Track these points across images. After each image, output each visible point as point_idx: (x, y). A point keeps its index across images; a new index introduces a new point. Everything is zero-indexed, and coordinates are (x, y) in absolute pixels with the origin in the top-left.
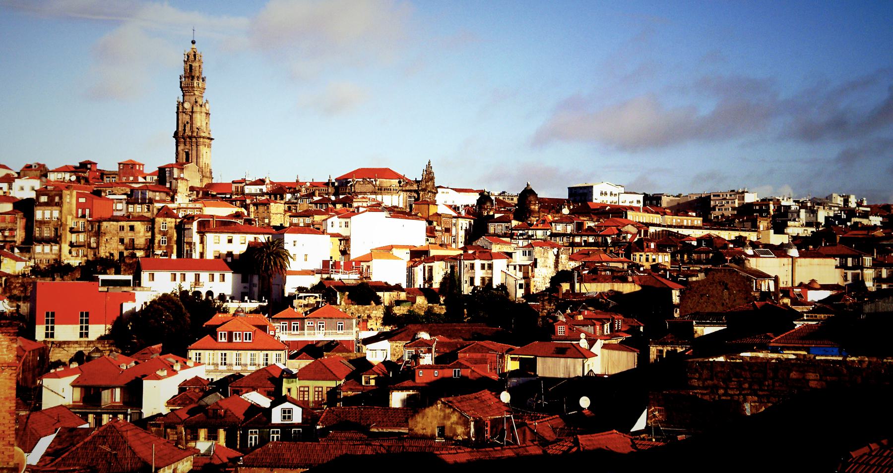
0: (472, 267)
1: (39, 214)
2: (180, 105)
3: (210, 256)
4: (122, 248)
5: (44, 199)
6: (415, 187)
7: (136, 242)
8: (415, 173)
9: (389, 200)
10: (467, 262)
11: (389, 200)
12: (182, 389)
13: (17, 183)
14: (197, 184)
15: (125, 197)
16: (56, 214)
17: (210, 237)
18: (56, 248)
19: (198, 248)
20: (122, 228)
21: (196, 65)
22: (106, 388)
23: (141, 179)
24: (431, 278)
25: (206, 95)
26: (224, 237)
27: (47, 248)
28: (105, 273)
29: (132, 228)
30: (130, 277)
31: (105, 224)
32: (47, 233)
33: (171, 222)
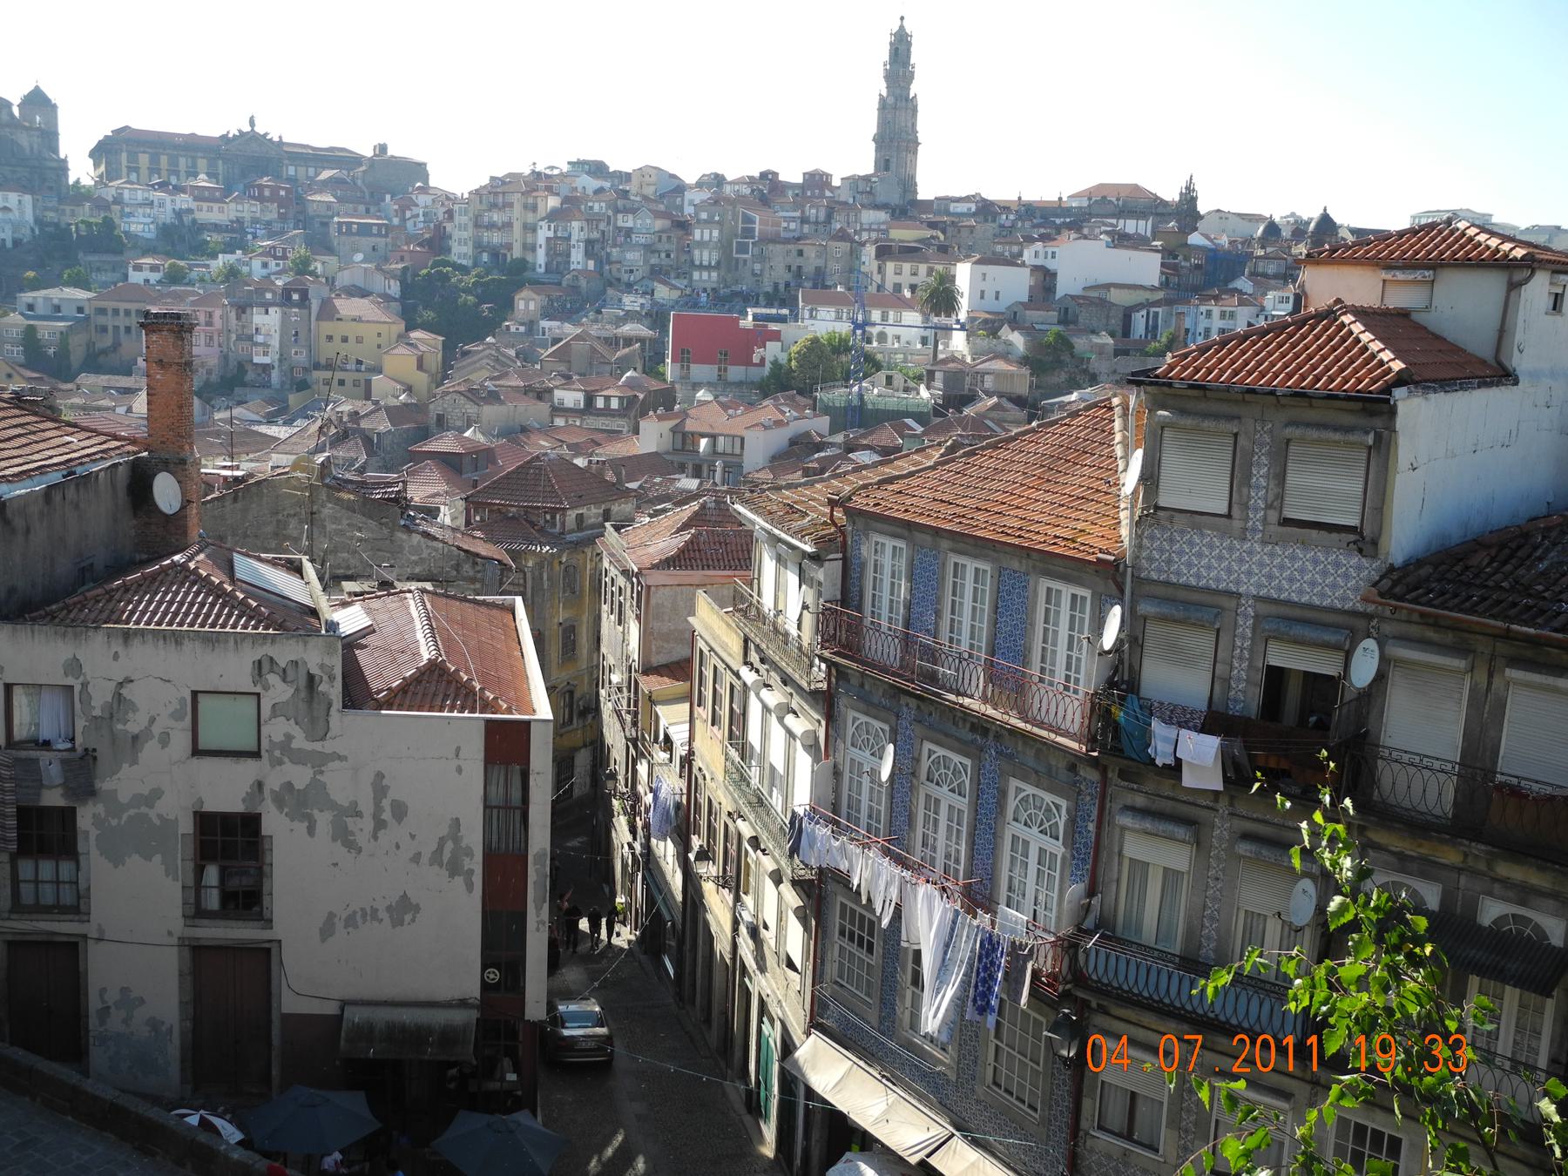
0: (1209, 314)
1: (697, 234)
2: (882, 100)
3: (889, 286)
4: (788, 277)
5: (704, 216)
6: (1169, 210)
7: (805, 270)
8: (1170, 193)
9: (1130, 226)
10: (1203, 309)
11: (1130, 226)
12: (793, 442)
13: (688, 195)
14: (895, 199)
15: (798, 214)
16: (716, 233)
17: (890, 266)
18: (714, 274)
19: (877, 278)
20: (788, 252)
21: (902, 48)
22: (703, 436)
23: (828, 194)
24: (1155, 327)
25: (914, 89)
26: (907, 267)
27: (705, 275)
28: (769, 305)
29: (800, 253)
30: (785, 311)
31: (771, 247)
32: (705, 256)
33: (845, 246)
